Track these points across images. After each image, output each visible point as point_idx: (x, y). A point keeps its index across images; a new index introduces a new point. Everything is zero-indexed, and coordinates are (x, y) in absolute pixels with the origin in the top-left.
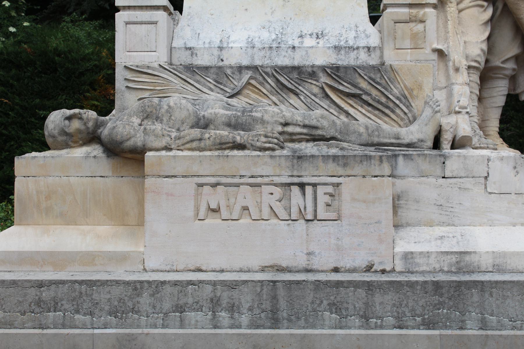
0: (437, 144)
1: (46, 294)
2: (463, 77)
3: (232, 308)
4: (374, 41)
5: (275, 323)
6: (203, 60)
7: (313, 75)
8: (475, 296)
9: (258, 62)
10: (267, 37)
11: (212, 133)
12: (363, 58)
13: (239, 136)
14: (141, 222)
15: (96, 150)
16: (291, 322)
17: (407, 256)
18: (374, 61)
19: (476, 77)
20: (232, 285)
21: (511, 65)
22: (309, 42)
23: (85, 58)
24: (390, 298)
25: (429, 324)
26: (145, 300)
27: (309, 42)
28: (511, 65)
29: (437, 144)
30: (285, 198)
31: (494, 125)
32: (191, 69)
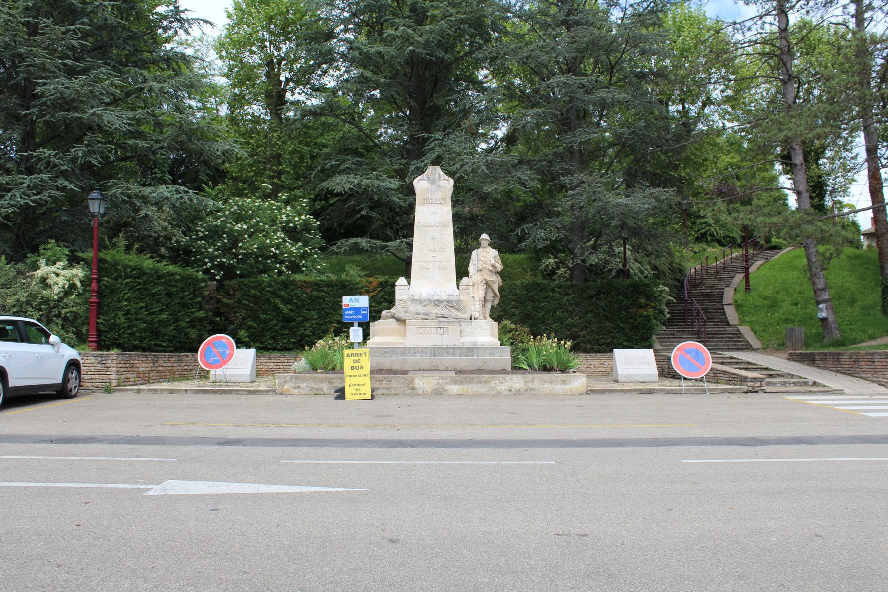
0: (471, 319)
1: (386, 350)
2: (478, 303)
3: (426, 353)
4: (458, 293)
5: (435, 356)
6: (416, 298)
7: (443, 302)
8: (476, 350)
9: (430, 298)
10: (431, 292)
11: (421, 316)
12: (455, 298)
13: (427, 317)
14: (405, 336)
15: (394, 320)
16: (438, 356)
17: (463, 343)
18: (458, 298)
19: (481, 302)
20: (426, 348)
21: (492, 299)
22: (442, 293)
23: (358, 283)
24: (458, 351)
25: (466, 356)
26: (407, 351)
27: (442, 293)
28: (492, 299)
29: (471, 319)
30: (437, 330)
31: (488, 314)
32: (414, 301)
